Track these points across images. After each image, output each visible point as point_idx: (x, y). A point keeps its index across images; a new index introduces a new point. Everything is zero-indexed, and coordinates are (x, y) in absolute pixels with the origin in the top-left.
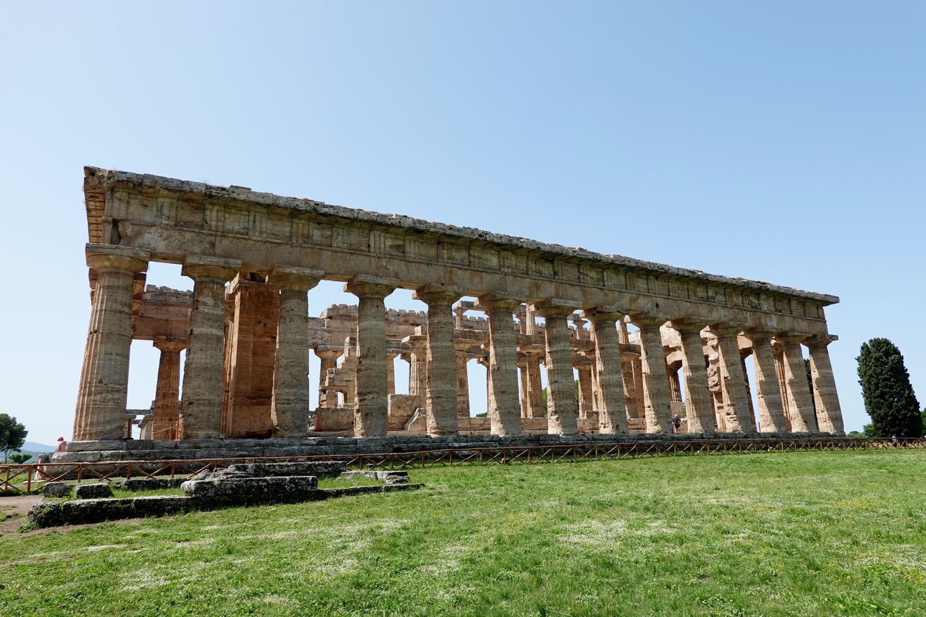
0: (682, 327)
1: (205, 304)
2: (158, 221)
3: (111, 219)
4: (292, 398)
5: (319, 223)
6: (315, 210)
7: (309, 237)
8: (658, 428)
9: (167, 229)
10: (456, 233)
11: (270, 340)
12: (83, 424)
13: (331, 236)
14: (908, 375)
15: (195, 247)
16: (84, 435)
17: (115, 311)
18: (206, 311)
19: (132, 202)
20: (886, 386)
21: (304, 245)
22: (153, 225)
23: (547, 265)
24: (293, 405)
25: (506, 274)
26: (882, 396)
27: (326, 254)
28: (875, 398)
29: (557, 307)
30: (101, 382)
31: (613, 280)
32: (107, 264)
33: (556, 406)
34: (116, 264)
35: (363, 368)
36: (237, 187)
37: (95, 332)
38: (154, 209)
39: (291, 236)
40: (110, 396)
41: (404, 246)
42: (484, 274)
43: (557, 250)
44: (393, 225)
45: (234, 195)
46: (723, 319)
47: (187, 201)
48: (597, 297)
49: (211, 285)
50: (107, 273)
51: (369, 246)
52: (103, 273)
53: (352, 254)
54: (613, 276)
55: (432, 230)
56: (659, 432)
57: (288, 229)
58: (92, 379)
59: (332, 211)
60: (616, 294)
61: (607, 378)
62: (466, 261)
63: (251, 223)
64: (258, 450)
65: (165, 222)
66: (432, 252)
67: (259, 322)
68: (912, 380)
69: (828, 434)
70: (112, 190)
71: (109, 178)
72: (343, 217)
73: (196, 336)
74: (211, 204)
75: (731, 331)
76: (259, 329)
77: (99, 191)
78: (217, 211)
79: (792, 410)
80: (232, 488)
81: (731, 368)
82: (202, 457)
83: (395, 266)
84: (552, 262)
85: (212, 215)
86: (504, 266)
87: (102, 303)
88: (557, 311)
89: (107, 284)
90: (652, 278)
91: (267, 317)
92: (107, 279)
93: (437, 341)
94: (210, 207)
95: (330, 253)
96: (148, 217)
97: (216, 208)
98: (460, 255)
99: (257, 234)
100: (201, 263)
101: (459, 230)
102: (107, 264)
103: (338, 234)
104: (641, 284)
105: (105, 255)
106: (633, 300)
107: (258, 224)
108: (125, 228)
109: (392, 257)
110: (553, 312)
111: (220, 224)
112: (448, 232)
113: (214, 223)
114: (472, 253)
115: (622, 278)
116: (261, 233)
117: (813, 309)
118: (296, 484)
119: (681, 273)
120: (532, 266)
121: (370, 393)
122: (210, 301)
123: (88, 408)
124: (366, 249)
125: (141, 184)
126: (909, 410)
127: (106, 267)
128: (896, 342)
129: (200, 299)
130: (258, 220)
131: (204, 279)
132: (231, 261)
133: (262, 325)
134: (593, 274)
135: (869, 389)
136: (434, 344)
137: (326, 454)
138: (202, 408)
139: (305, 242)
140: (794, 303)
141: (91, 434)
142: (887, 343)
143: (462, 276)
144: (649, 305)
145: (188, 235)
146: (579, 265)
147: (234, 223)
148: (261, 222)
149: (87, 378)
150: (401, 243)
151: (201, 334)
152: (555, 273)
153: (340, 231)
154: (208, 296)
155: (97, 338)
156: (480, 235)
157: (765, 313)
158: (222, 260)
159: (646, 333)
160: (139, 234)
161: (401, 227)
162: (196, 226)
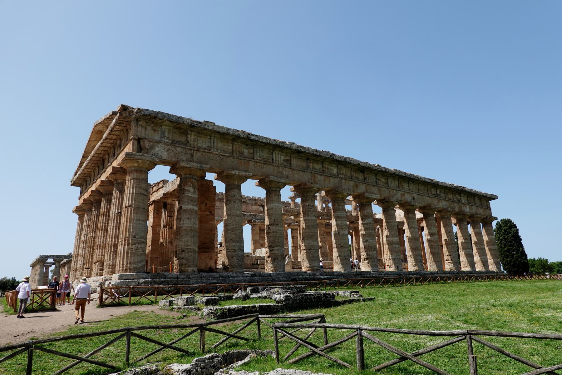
0: (425, 211)
1: (189, 191)
2: (162, 140)
3: (137, 138)
4: (237, 248)
5: (247, 145)
6: (248, 137)
7: (241, 153)
8: (416, 268)
9: (167, 145)
10: (319, 154)
11: (209, 213)
12: (125, 263)
13: (253, 153)
14: (521, 239)
15: (183, 157)
16: (126, 270)
17: (141, 194)
18: (190, 195)
19: (148, 127)
20: (510, 246)
21: (240, 158)
22: (159, 142)
23: (361, 174)
24: (237, 253)
25: (341, 178)
26: (508, 251)
27: (251, 163)
28: (504, 252)
29: (367, 198)
30: (134, 237)
31: (393, 183)
32: (136, 165)
33: (367, 255)
34: (141, 165)
35: (271, 231)
36: (208, 122)
37: (129, 206)
38: (160, 132)
39: (233, 152)
40: (140, 246)
41: (290, 160)
42: (331, 178)
43: (368, 165)
44: (287, 148)
45: (206, 127)
46: (445, 207)
47: (178, 128)
48: (386, 193)
49: (192, 180)
50: (135, 170)
51: (273, 159)
52: (132, 170)
53: (265, 164)
54: (392, 181)
55: (307, 151)
56: (417, 270)
57: (231, 148)
58: (129, 235)
59: (256, 139)
60: (395, 191)
61: (391, 239)
62: (321, 170)
63: (212, 143)
64: (222, 280)
65: (166, 141)
66: (304, 164)
67: (203, 203)
68: (523, 242)
69: (494, 272)
70: (137, 120)
71: (137, 113)
72: (262, 142)
73: (184, 210)
74: (191, 131)
75: (449, 214)
77: (127, 120)
78: (194, 135)
79: (476, 258)
80: (299, 299)
81: (449, 234)
82: (193, 284)
83: (286, 172)
84: (363, 172)
85: (191, 137)
86: (340, 174)
87: (133, 188)
88: (367, 200)
89: (135, 177)
90: (411, 183)
92: (135, 174)
93: (308, 216)
94: (190, 132)
95: (253, 163)
96: (157, 137)
97: (193, 133)
98: (318, 166)
99: (215, 150)
100: (188, 166)
101: (320, 152)
102: (136, 165)
103: (257, 152)
104: (406, 186)
105: (136, 159)
106: (403, 195)
107: (215, 144)
108: (144, 144)
109: (285, 167)
110: (364, 201)
111: (196, 143)
112: (315, 153)
113: (192, 143)
114: (324, 165)
115: (397, 182)
116: (217, 149)
117: (485, 203)
118: (326, 297)
119: (426, 180)
120: (354, 174)
121: (276, 246)
123: (127, 253)
124: (271, 161)
125: (155, 117)
126: (522, 259)
127: (134, 167)
128: (514, 221)
129: (186, 188)
130: (215, 141)
131: (187, 176)
132: (204, 166)
133: (204, 204)
135: (501, 247)
136: (305, 218)
137: (258, 282)
138: (190, 254)
139: (240, 156)
140: (476, 199)
141: (130, 269)
142: (510, 221)
143: (320, 178)
144: (410, 198)
145: (179, 149)
146: (376, 174)
147: (203, 143)
148: (217, 143)
149: (126, 234)
150: (288, 158)
151: (187, 209)
152: (365, 179)
153: (258, 150)
154: (190, 186)
155: (131, 210)
156: (331, 156)
157: (464, 204)
158: (199, 165)
159: (408, 214)
160: (152, 147)
161: (291, 149)
162: (183, 144)
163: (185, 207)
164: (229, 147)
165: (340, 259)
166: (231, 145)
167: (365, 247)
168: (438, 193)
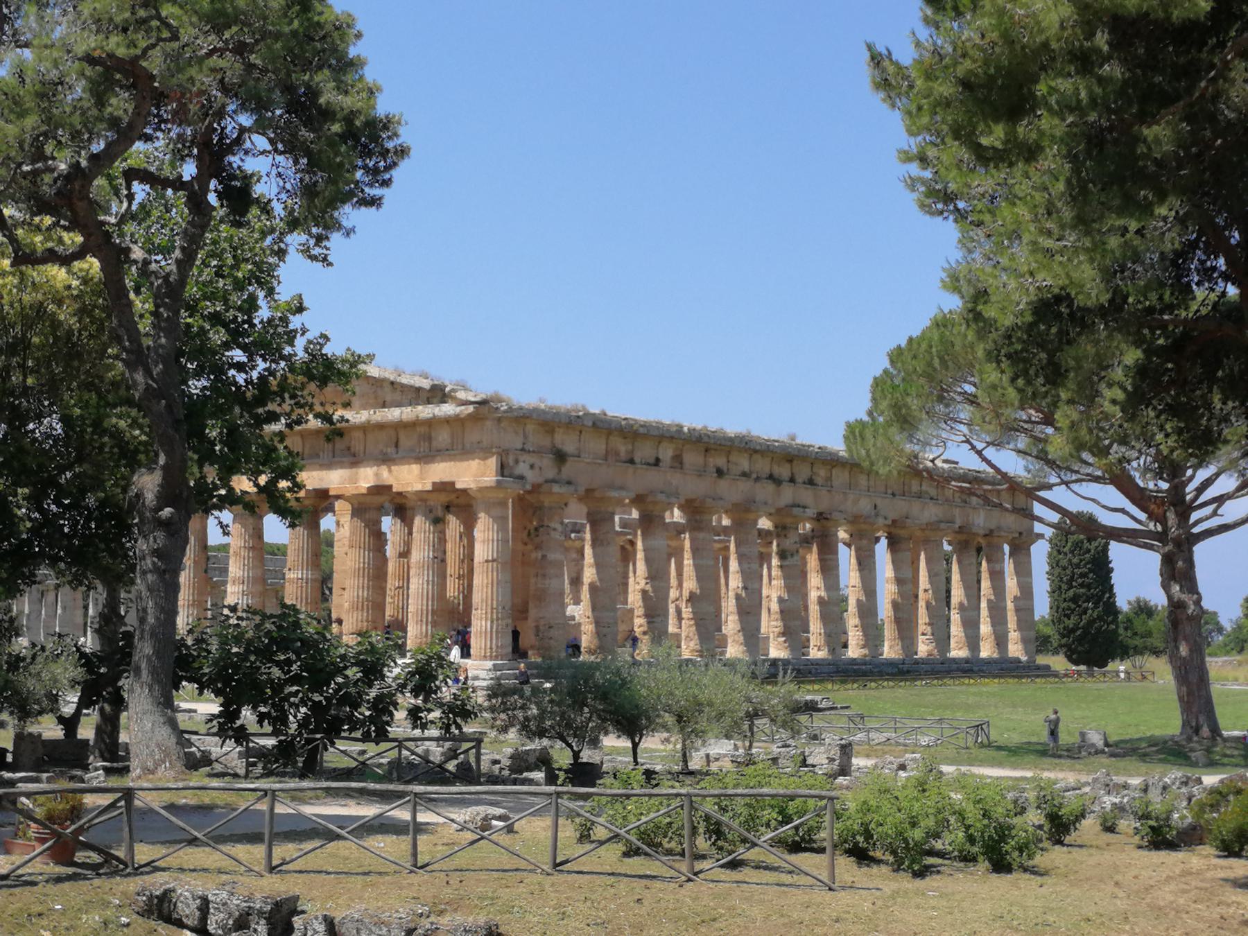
8: (865, 651)
14: (1112, 570)
20: (1082, 585)
26: (1075, 599)
28: (1065, 600)
56: (865, 656)
57: (604, 447)
69: (1018, 661)
79: (985, 628)
84: (790, 461)
115: (847, 474)
126: (1105, 621)
135: (1060, 587)
165: (744, 635)
167: (782, 612)
168: (924, 488)
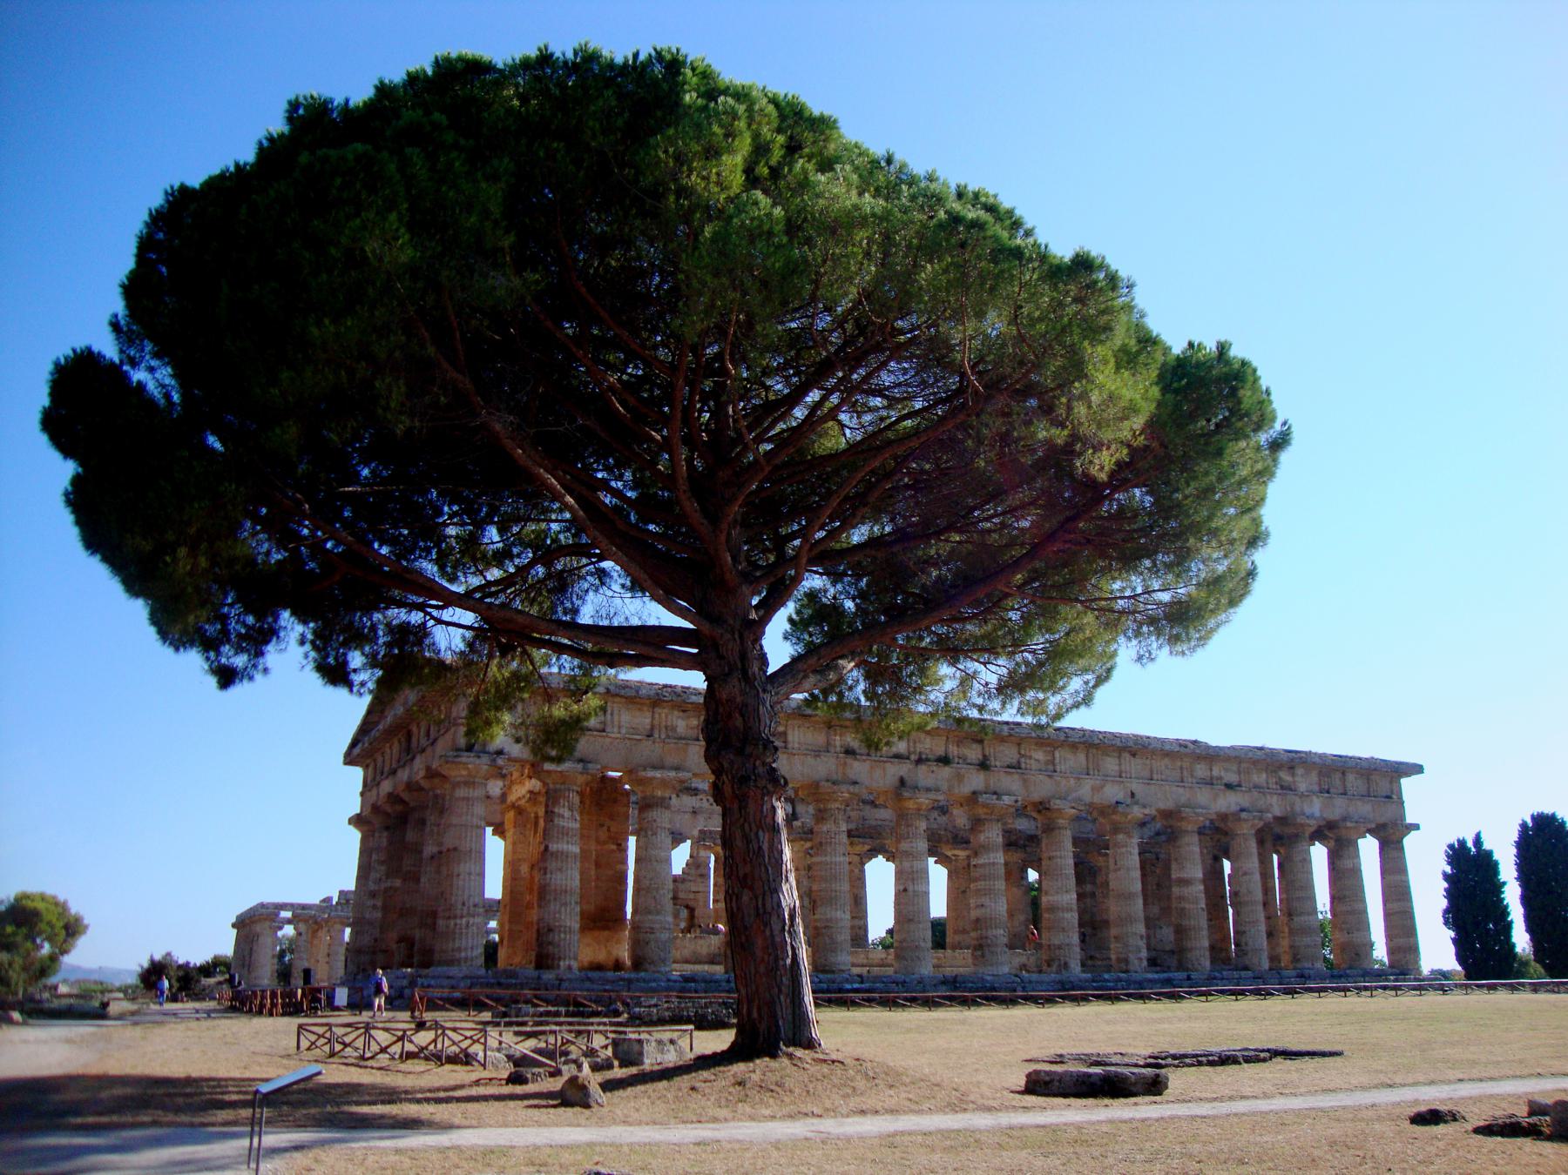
29: (985, 806)
32: (464, 773)
39: (652, 729)
54: (1069, 756)
57: (648, 721)
60: (1072, 781)
66: (819, 738)
76: (603, 834)
91: (611, 817)
102: (464, 773)
107: (616, 718)
110: (981, 811)
115: (1081, 757)
122: (567, 814)
134: (1040, 755)
140: (1350, 777)
157: (1302, 796)
163: (554, 847)
164: (643, 720)
166: (649, 714)
